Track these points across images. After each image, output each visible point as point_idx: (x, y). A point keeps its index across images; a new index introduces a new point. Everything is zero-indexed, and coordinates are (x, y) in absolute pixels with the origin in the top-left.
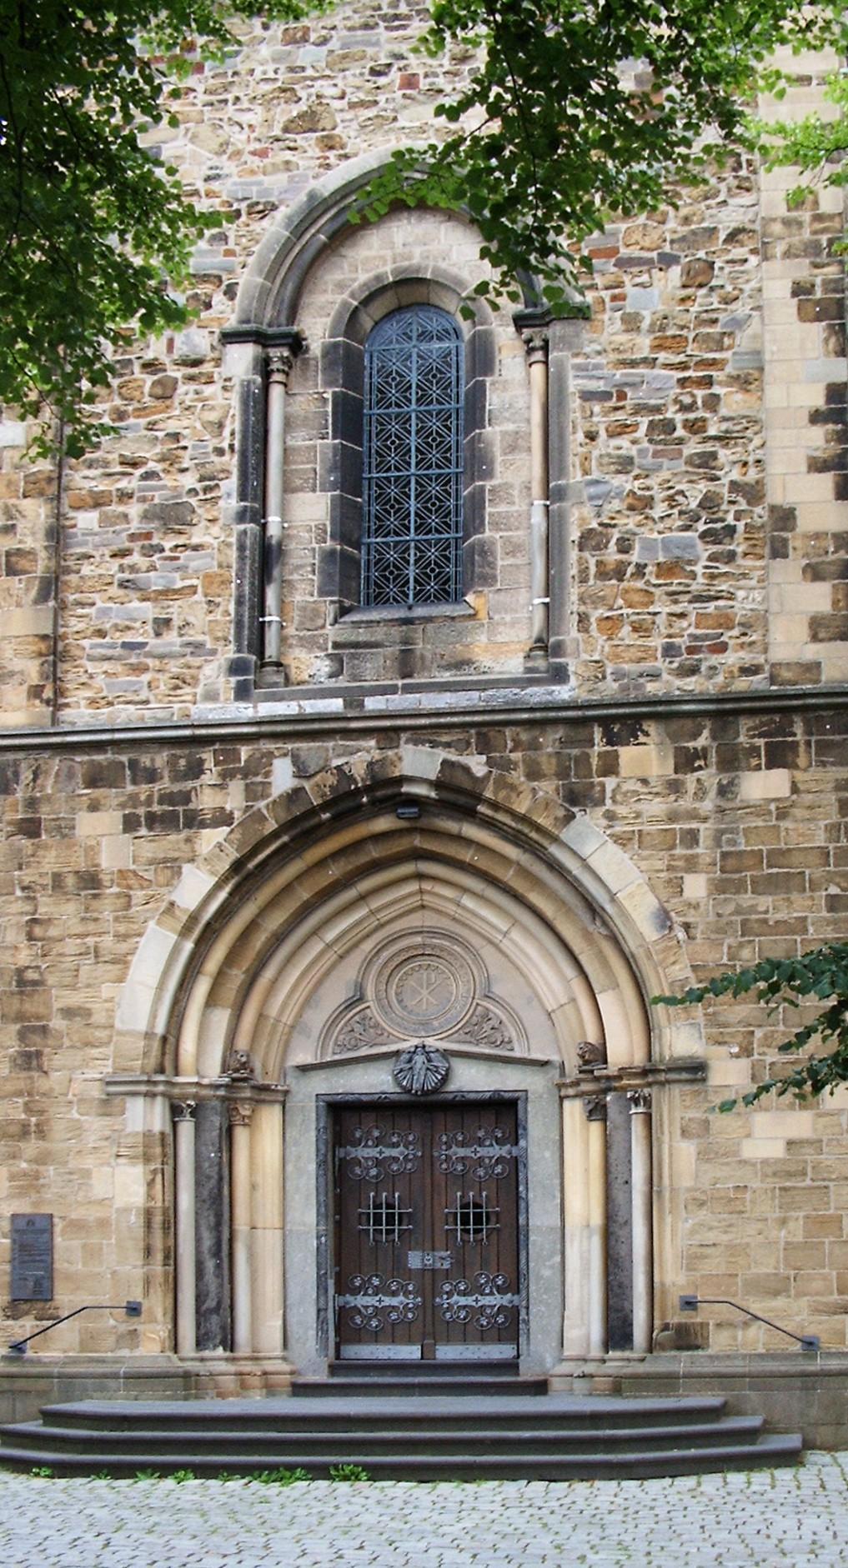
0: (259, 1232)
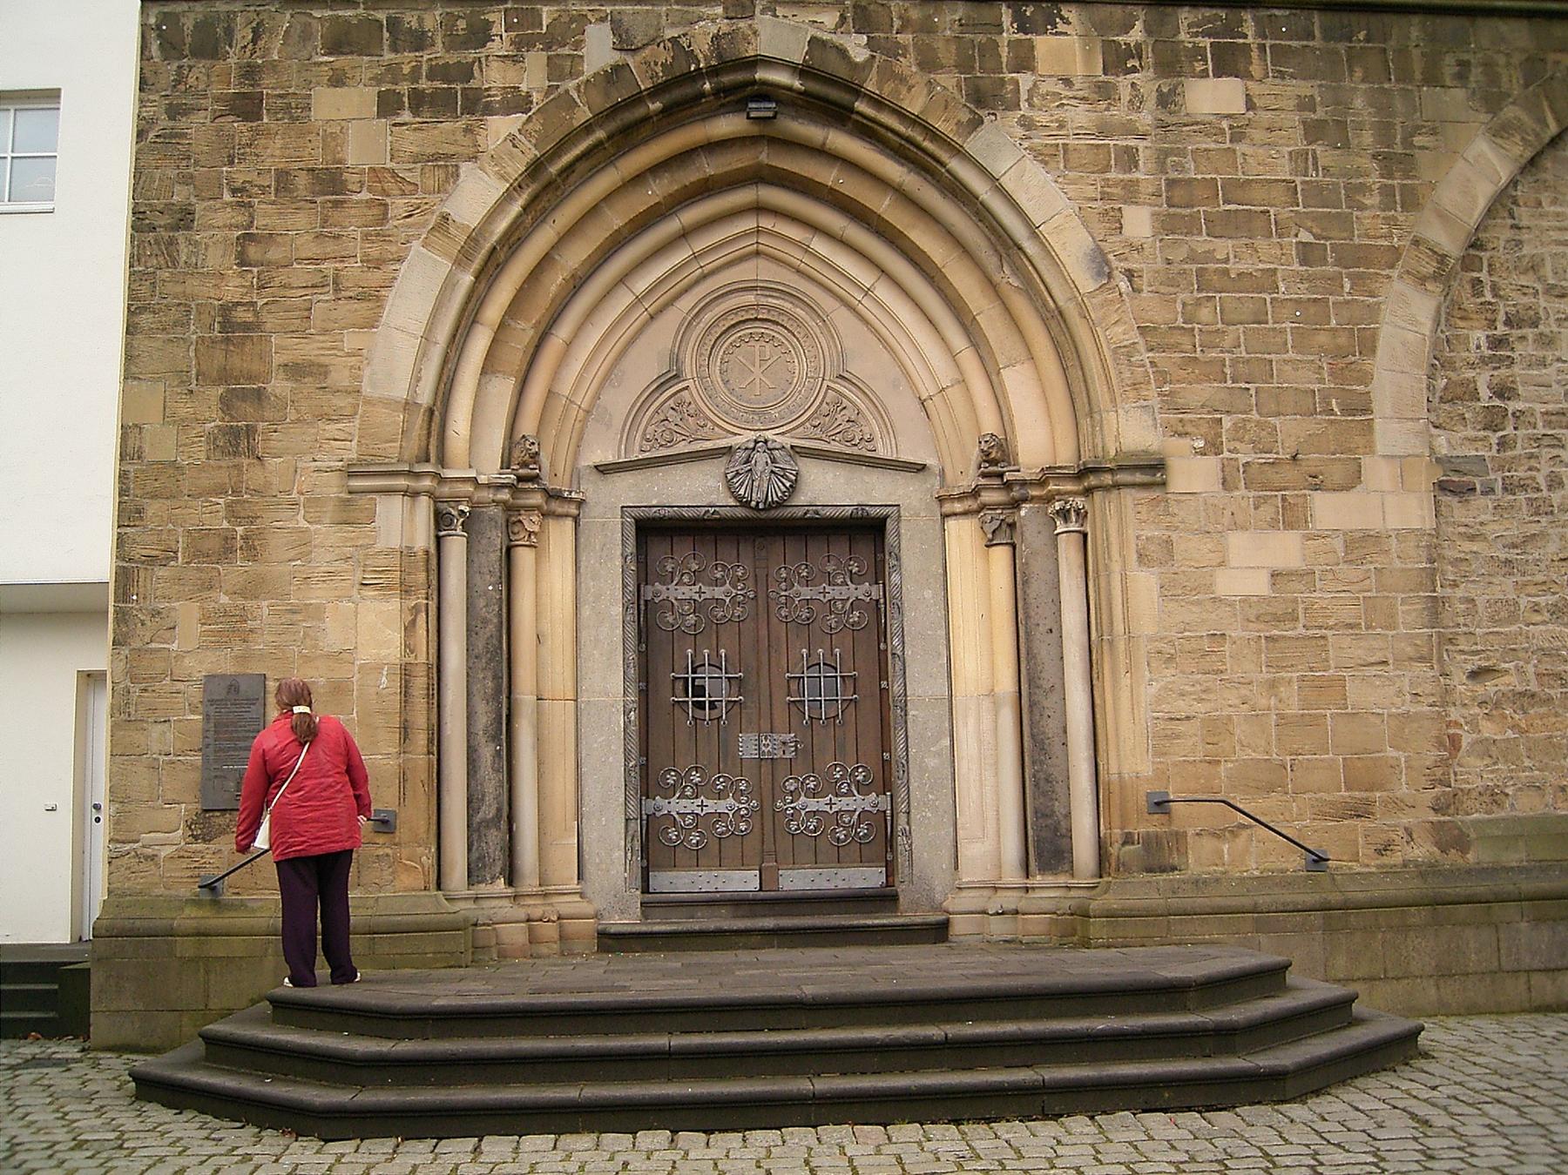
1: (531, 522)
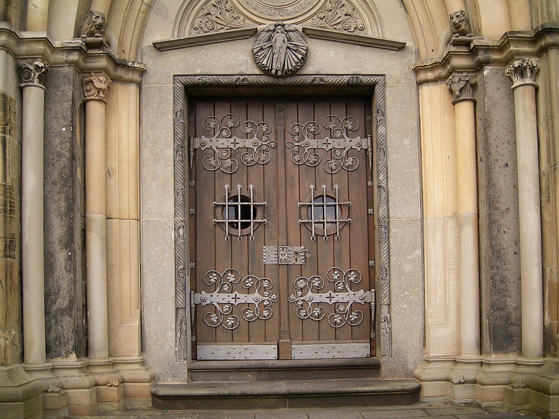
0: (114, 222)
1: (100, 81)
